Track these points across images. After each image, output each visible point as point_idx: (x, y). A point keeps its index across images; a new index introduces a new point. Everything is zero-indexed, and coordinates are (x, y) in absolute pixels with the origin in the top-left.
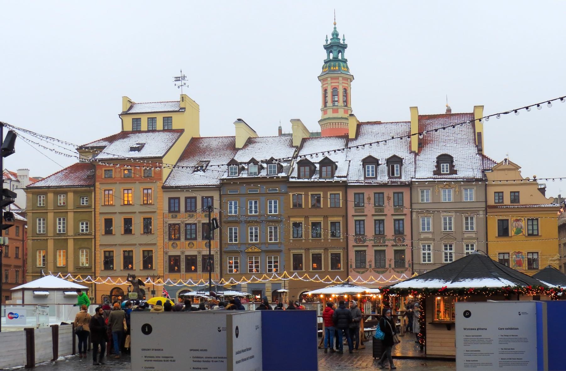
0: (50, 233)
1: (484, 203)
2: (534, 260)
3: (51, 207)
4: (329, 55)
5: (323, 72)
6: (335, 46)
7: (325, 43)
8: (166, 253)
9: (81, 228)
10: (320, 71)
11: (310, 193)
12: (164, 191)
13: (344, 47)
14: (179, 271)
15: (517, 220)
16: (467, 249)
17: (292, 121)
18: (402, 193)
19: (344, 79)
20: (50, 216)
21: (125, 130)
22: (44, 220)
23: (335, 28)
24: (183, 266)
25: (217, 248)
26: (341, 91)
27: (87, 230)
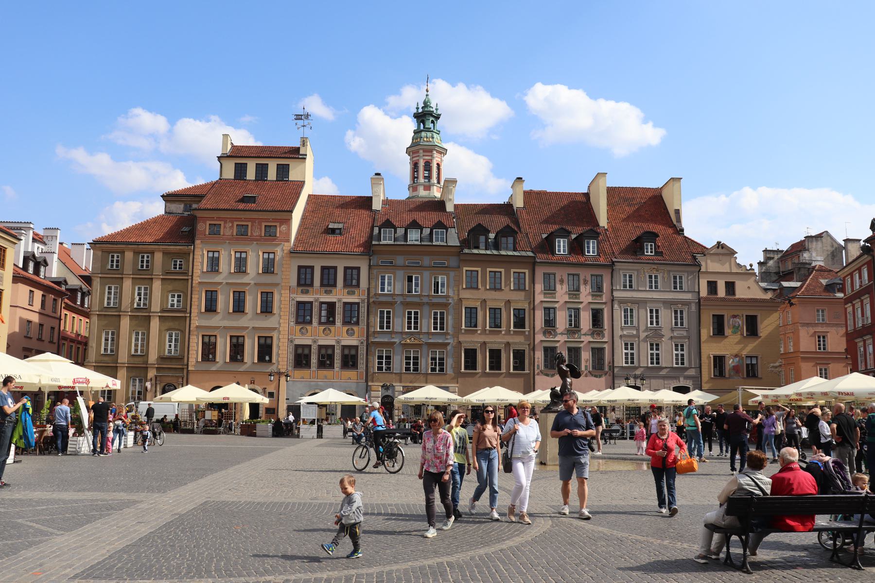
1: (696, 294)
2: (752, 365)
3: (128, 269)
4: (419, 126)
7: (415, 111)
8: (292, 341)
9: (170, 302)
10: (409, 143)
12: (291, 257)
13: (437, 117)
14: (308, 365)
15: (735, 316)
16: (652, 349)
18: (601, 276)
24: (314, 360)
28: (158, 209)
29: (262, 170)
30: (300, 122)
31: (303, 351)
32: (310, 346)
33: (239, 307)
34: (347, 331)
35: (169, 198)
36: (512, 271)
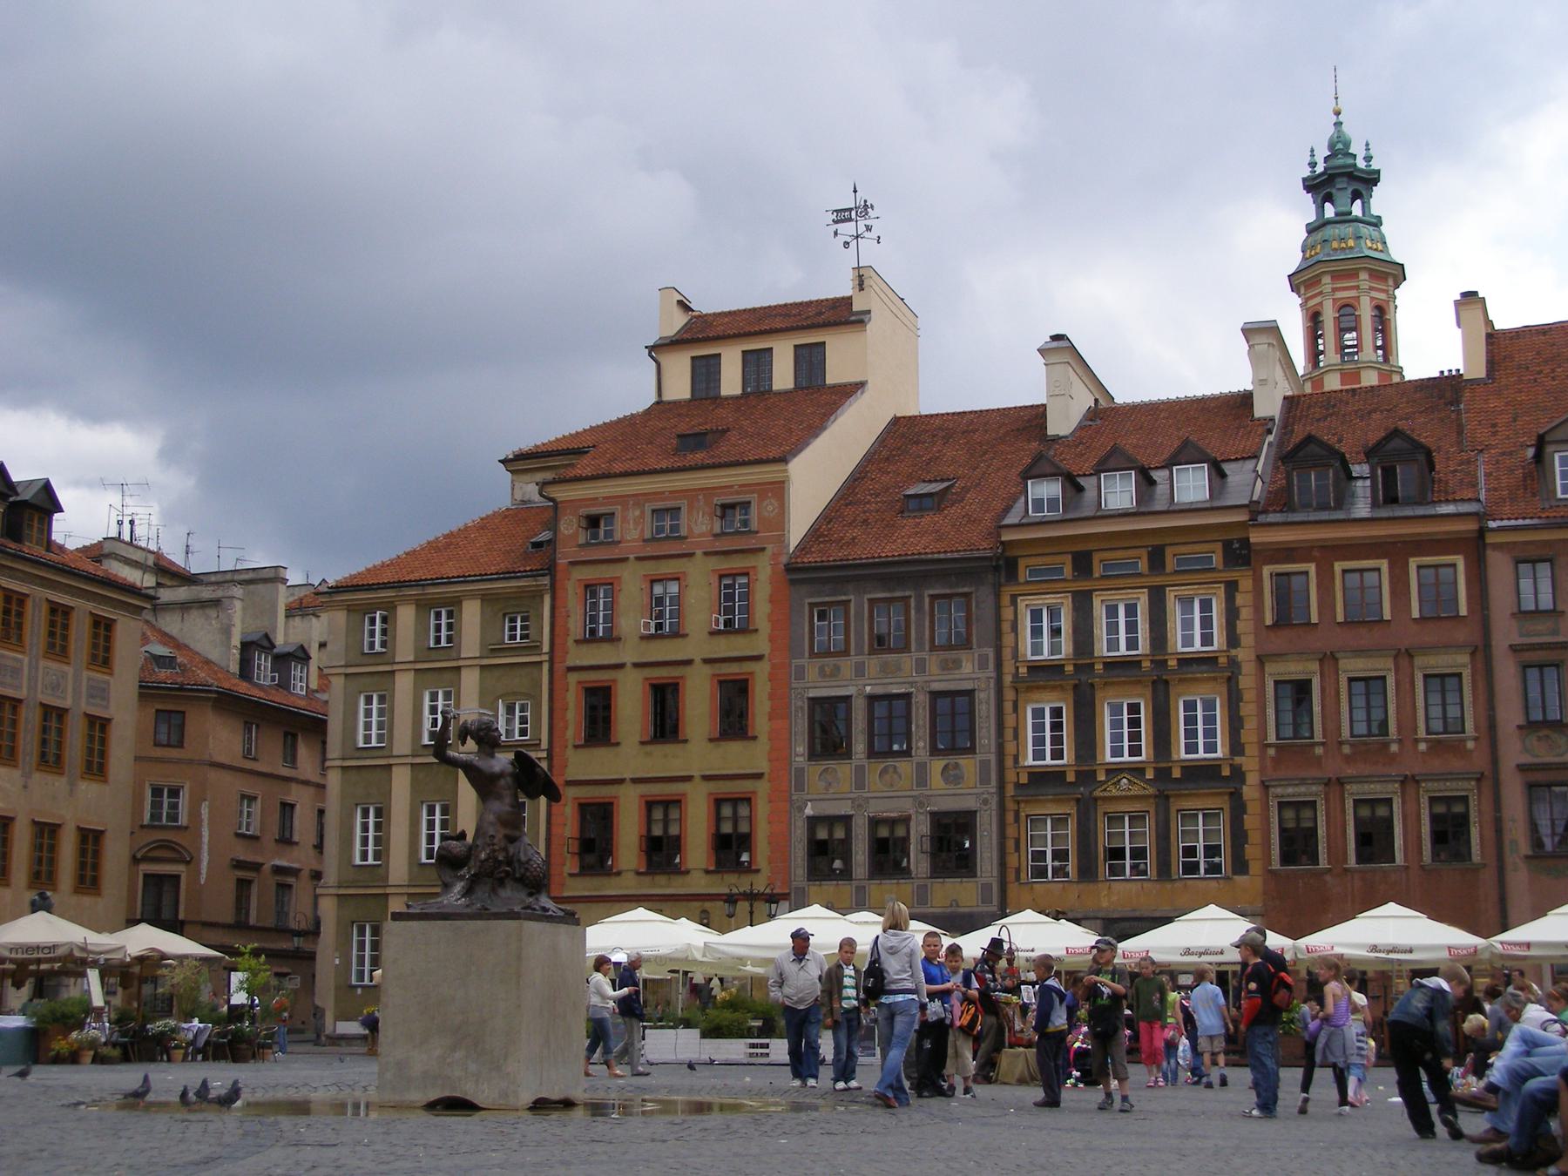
0: (402, 744)
3: (405, 649)
5: (1304, 258)
6: (1341, 180)
7: (1307, 172)
10: (1294, 260)
11: (1338, 567)
12: (793, 582)
13: (1372, 179)
17: (1250, 331)
19: (1377, 276)
20: (404, 684)
21: (667, 397)
22: (382, 699)
23: (1338, 124)
25: (988, 782)
26: (1366, 313)
27: (523, 732)
28: (500, 491)
29: (757, 364)
30: (848, 229)
31: (892, 832)
32: (850, 817)
33: (665, 723)
34: (946, 768)
35: (521, 465)
36: (1413, 563)
